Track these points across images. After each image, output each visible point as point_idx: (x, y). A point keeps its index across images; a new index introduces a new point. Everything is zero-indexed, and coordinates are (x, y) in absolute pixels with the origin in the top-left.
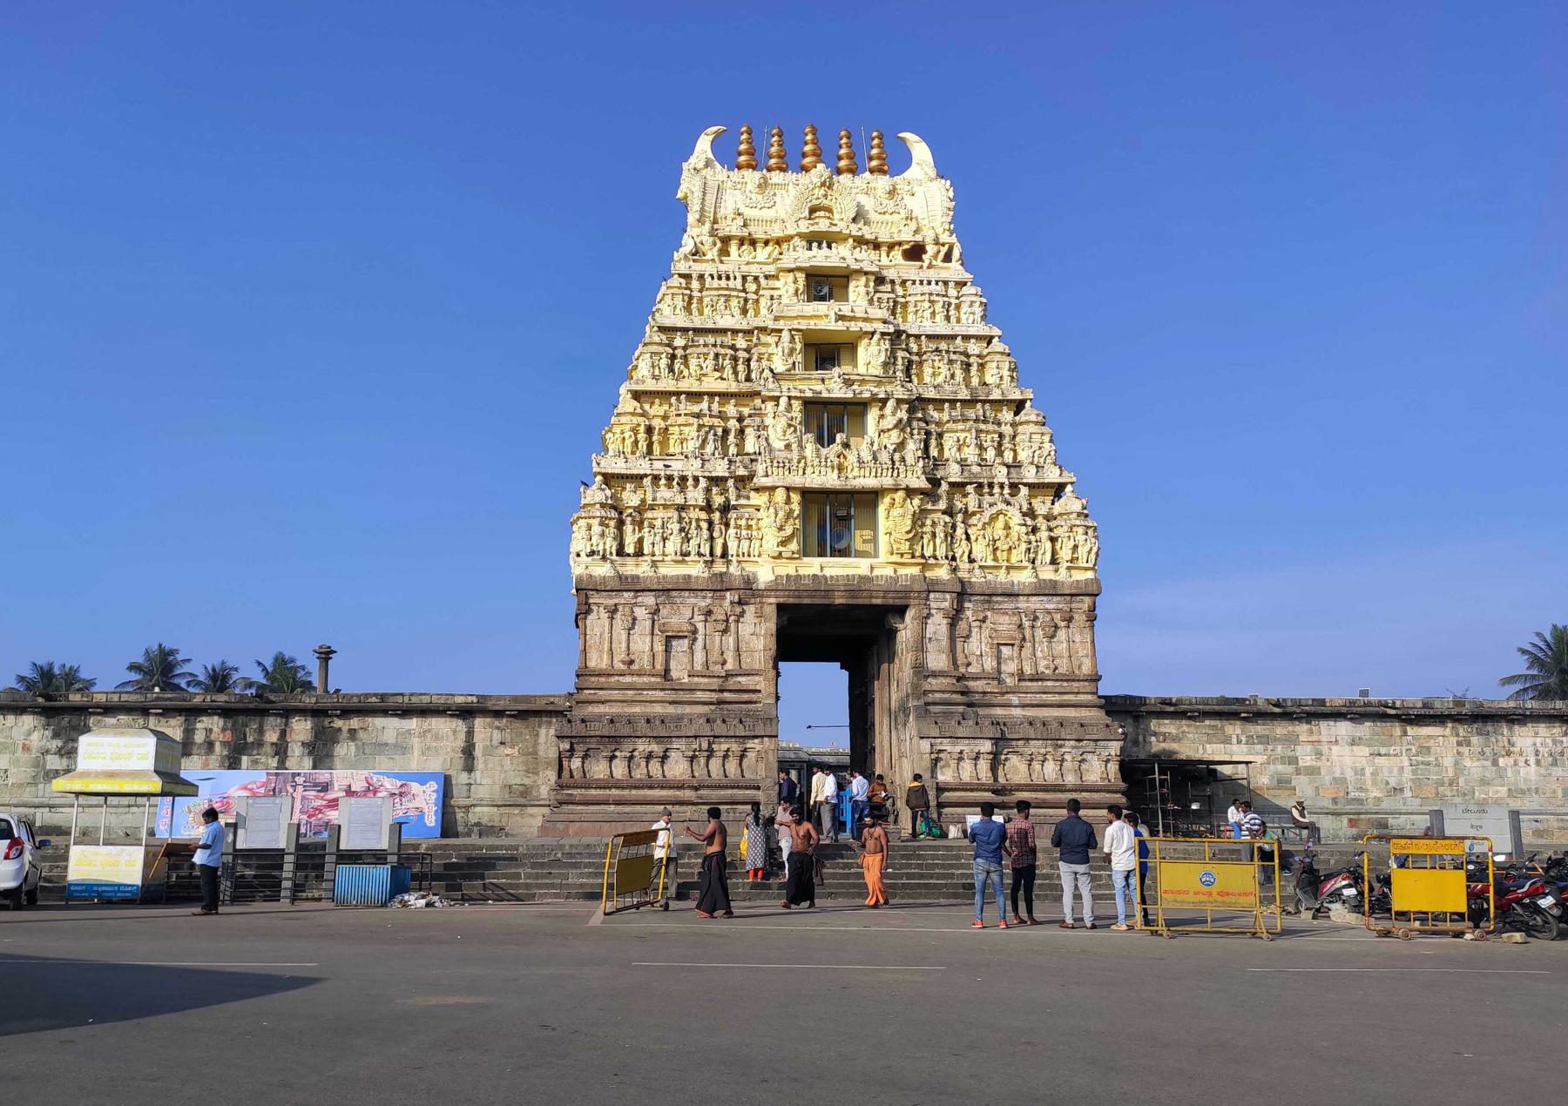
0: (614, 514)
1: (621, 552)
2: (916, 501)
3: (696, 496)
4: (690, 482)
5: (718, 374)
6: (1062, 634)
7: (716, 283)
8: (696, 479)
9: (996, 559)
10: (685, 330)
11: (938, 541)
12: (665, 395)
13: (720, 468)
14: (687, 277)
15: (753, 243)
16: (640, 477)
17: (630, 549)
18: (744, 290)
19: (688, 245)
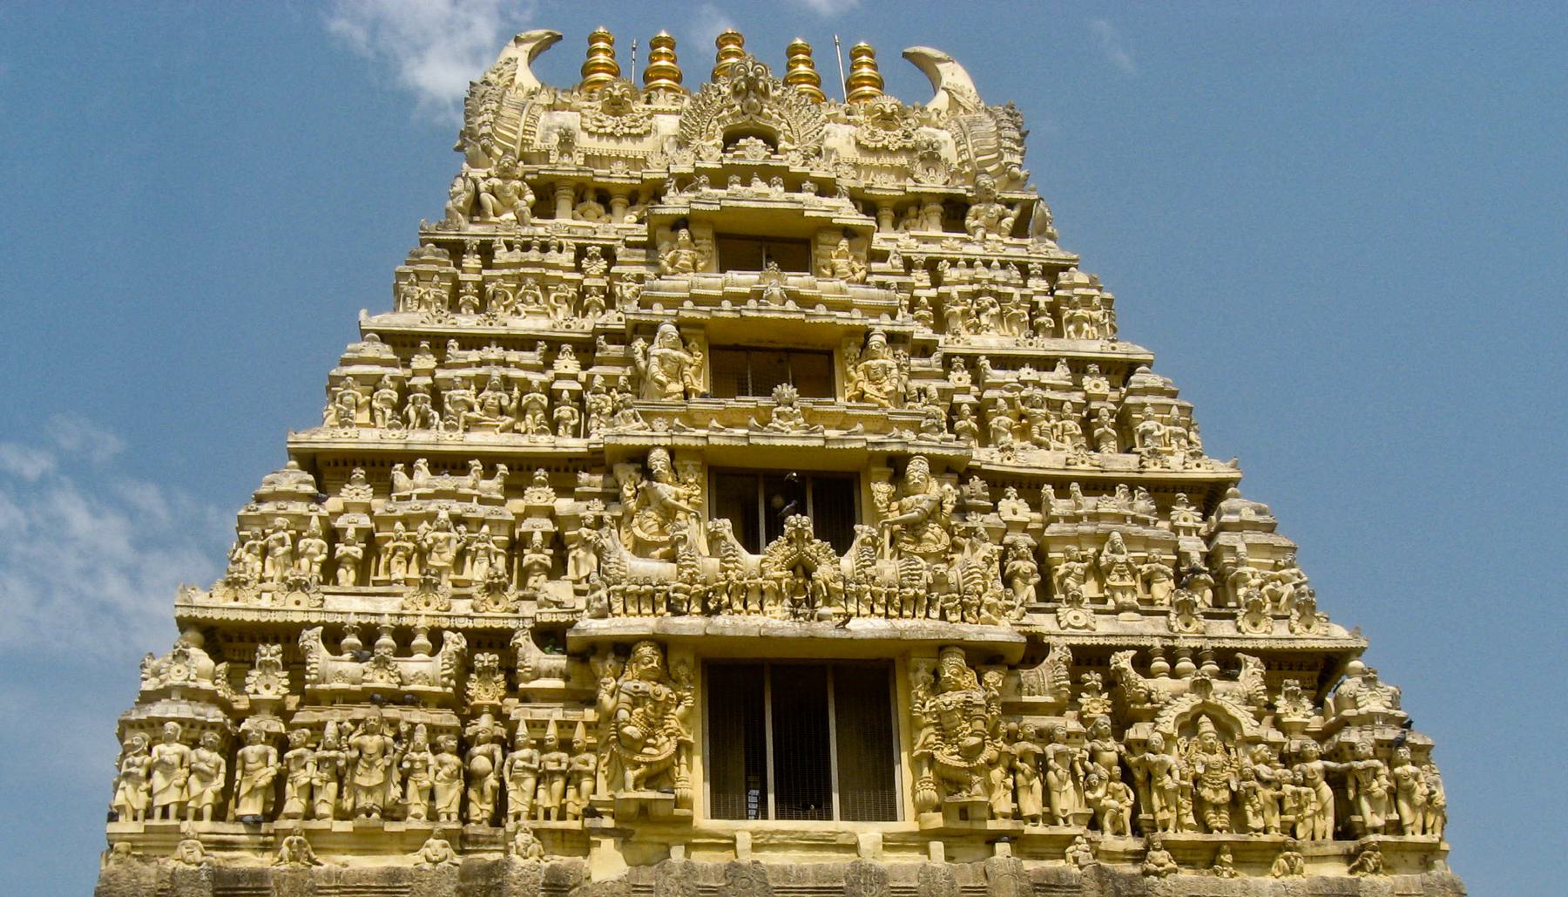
4: (421, 640)
8: (436, 637)
15: (604, 198)
16: (287, 635)
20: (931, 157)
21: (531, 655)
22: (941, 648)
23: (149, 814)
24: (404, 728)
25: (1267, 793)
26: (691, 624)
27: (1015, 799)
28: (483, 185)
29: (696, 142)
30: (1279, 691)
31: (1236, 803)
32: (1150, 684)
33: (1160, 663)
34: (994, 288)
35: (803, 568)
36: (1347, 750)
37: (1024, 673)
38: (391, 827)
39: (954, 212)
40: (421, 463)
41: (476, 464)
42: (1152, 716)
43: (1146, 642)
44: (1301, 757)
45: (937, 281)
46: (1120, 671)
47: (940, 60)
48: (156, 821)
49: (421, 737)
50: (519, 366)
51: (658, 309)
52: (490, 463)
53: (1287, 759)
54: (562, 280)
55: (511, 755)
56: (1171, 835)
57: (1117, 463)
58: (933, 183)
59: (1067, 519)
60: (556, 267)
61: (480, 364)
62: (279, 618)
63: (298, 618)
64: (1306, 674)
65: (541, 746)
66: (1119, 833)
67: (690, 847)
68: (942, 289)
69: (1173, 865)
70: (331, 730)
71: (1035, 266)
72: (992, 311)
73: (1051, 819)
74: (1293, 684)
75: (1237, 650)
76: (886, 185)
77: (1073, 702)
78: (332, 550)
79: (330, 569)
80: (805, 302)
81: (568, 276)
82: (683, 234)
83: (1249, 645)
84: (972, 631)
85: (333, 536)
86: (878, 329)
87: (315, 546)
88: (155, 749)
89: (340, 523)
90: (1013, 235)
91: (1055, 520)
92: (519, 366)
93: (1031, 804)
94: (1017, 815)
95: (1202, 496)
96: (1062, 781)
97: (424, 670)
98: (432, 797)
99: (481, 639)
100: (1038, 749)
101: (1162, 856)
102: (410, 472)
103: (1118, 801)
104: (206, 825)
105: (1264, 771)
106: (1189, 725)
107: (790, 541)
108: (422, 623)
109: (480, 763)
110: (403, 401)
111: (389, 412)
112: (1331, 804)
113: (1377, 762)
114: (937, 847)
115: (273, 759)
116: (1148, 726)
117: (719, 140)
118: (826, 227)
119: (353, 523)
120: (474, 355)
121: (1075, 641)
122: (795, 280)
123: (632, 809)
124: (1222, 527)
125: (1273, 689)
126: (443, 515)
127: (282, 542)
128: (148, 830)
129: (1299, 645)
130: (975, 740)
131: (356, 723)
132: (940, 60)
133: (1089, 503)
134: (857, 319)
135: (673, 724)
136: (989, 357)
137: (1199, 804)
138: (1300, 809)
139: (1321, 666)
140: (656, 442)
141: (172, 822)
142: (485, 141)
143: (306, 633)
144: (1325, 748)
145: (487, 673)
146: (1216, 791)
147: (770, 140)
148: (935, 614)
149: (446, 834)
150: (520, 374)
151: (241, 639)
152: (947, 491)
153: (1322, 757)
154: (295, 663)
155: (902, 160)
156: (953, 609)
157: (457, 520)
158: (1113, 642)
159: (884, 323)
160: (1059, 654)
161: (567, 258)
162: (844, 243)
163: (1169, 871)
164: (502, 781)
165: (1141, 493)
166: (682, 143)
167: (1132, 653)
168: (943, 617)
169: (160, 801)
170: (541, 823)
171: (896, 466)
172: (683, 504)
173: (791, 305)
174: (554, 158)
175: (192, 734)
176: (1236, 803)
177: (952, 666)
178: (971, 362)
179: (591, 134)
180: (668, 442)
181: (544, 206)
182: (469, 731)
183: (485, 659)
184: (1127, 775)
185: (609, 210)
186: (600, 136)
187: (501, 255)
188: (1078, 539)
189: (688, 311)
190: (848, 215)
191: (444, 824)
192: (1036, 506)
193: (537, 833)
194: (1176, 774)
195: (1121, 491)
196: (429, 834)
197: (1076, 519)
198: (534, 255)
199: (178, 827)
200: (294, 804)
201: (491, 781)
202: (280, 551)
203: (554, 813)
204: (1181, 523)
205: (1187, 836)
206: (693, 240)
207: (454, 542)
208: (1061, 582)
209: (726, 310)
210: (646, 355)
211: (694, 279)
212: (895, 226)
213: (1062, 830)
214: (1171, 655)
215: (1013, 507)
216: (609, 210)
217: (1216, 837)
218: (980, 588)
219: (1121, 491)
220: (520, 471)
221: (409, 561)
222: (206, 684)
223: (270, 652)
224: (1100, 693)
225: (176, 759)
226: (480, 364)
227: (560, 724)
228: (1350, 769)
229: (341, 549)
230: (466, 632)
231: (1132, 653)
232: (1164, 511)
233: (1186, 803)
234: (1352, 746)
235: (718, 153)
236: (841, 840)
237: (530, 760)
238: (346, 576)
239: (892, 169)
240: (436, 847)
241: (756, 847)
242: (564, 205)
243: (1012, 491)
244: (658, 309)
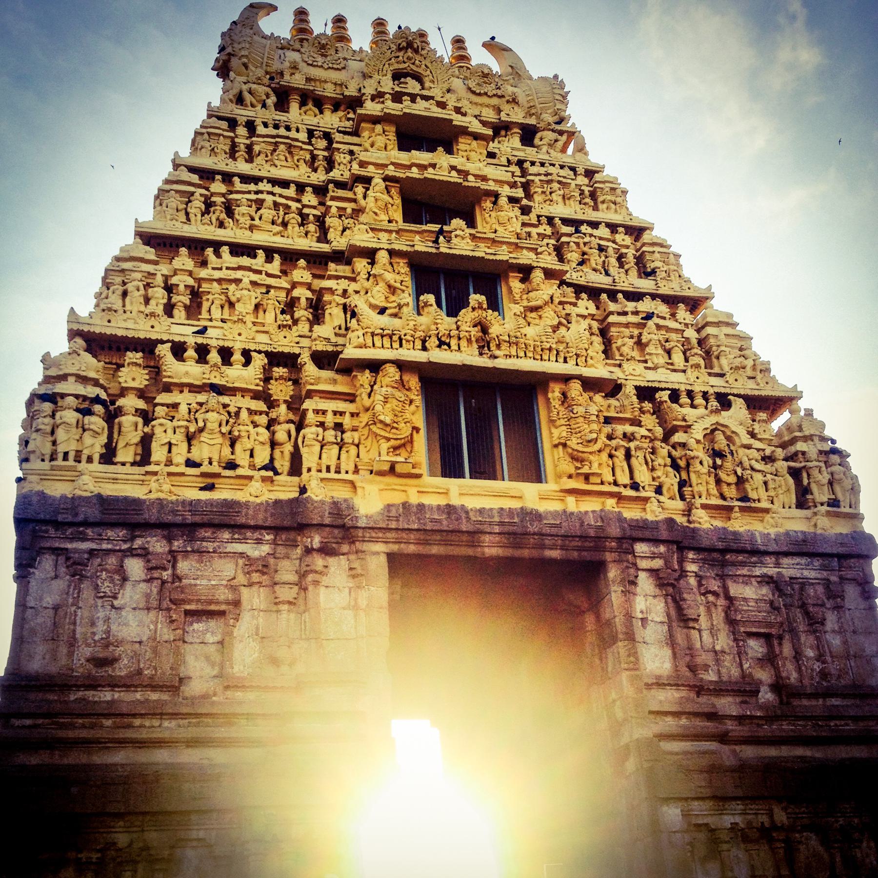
4: (237, 357)
16: (148, 347)
21: (310, 370)
22: (566, 379)
24: (232, 409)
25: (758, 477)
33: (684, 400)
40: (225, 249)
41: (261, 253)
42: (687, 429)
43: (676, 386)
48: (60, 462)
49: (244, 414)
50: (281, 196)
51: (371, 168)
52: (270, 252)
54: (302, 149)
58: (517, 116)
59: (619, 314)
60: (297, 140)
61: (257, 193)
62: (142, 336)
63: (154, 337)
65: (322, 425)
66: (672, 498)
70: (183, 409)
71: (580, 170)
79: (169, 309)
83: (736, 392)
85: (169, 289)
87: (159, 294)
88: (58, 415)
89: (174, 280)
91: (612, 313)
92: (281, 196)
94: (615, 483)
97: (240, 375)
98: (252, 456)
99: (275, 359)
102: (218, 255)
104: (96, 466)
105: (757, 466)
107: (474, 309)
112: (793, 487)
115: (140, 426)
118: (464, 131)
120: (252, 187)
123: (386, 467)
126: (246, 281)
129: (763, 393)
130: (594, 436)
131: (201, 404)
133: (631, 306)
134: (491, 186)
136: (561, 219)
137: (718, 481)
141: (71, 462)
142: (245, 60)
148: (561, 360)
150: (283, 201)
153: (786, 459)
155: (495, 101)
157: (254, 283)
158: (656, 385)
168: (565, 361)
170: (324, 475)
171: (525, 272)
172: (398, 285)
174: (287, 77)
178: (550, 220)
182: (273, 415)
185: (321, 112)
187: (261, 130)
188: (627, 325)
189: (391, 171)
193: (322, 480)
196: (250, 478)
197: (625, 313)
200: (158, 453)
203: (333, 469)
208: (618, 349)
209: (415, 173)
213: (643, 494)
214: (690, 394)
216: (321, 112)
220: (290, 257)
221: (222, 307)
222: (92, 375)
225: (74, 421)
226: (257, 193)
229: (175, 299)
230: (268, 354)
233: (712, 480)
234: (804, 453)
238: (180, 314)
242: (294, 106)
244: (371, 168)
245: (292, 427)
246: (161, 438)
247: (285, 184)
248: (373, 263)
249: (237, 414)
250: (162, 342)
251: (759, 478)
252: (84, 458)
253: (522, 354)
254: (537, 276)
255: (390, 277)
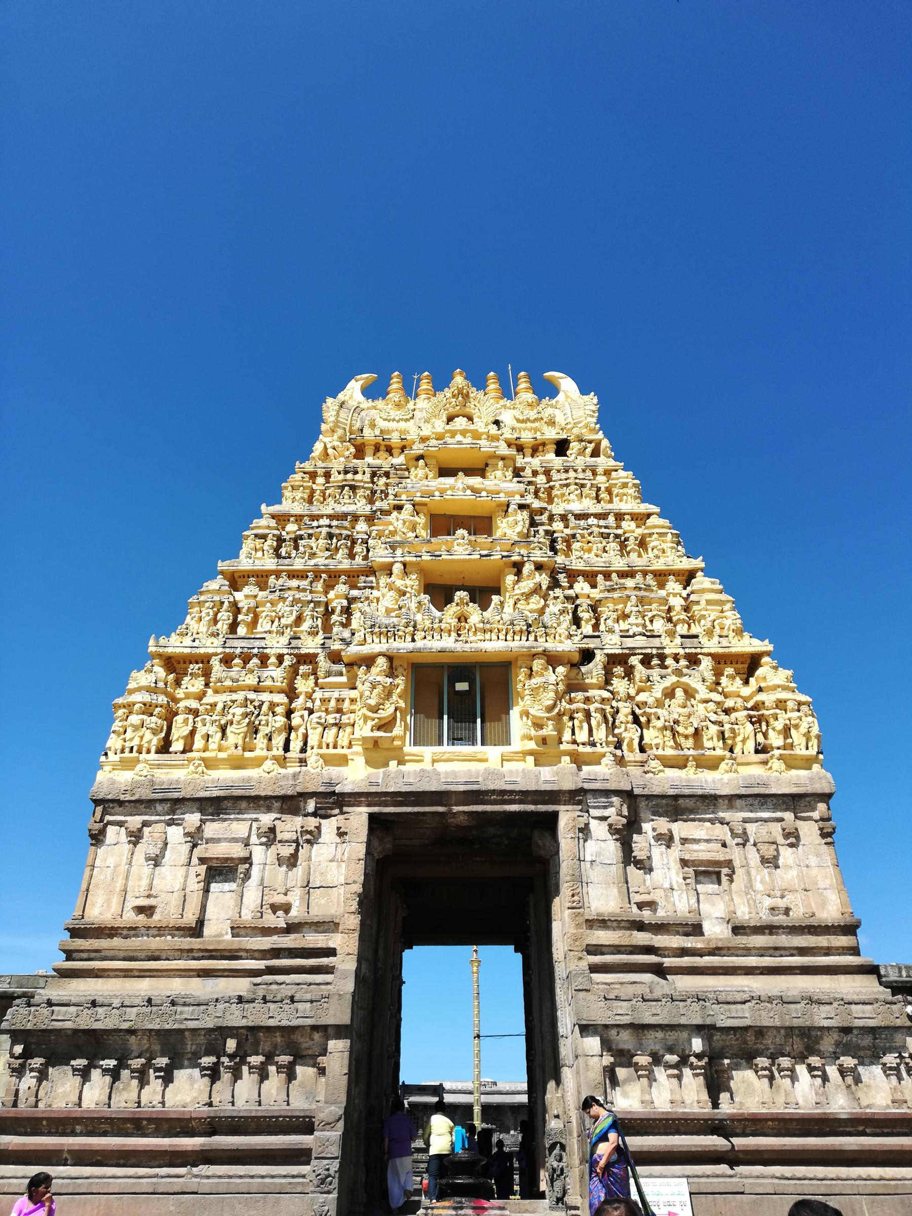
0: (162, 699)
1: (165, 747)
2: (561, 670)
3: (276, 674)
4: (273, 660)
5: (328, 554)
6: (787, 855)
7: (341, 477)
8: (280, 658)
9: (678, 746)
10: (299, 518)
11: (593, 722)
12: (261, 578)
13: (310, 645)
14: (313, 475)
16: (205, 660)
17: (177, 746)
18: (373, 483)
19: (318, 447)
20: (552, 423)
23: (123, 751)
24: (257, 704)
26: (403, 645)
27: (573, 733)
28: (328, 446)
29: (433, 420)
30: (723, 675)
31: (697, 733)
32: (649, 671)
33: (655, 662)
34: (577, 481)
35: (462, 618)
36: (761, 705)
37: (584, 669)
38: (247, 754)
39: (562, 447)
43: (649, 651)
44: (734, 709)
45: (549, 480)
46: (632, 667)
47: (561, 378)
48: (127, 754)
53: (727, 712)
54: (363, 487)
55: (311, 716)
56: (660, 752)
57: (636, 560)
58: (551, 434)
63: (211, 651)
64: (740, 666)
67: (401, 762)
68: (551, 484)
69: (662, 768)
71: (600, 470)
72: (577, 492)
73: (593, 744)
74: (729, 670)
75: (697, 654)
76: (527, 437)
77: (608, 682)
78: (235, 618)
80: (475, 491)
81: (366, 485)
82: (421, 462)
83: (705, 651)
84: (552, 645)
86: (513, 502)
87: (225, 616)
90: (592, 456)
93: (582, 736)
94: (574, 742)
95: (684, 578)
96: (599, 725)
98: (270, 739)
100: (586, 707)
101: (655, 764)
103: (631, 734)
104: (153, 756)
106: (670, 694)
107: (457, 604)
108: (273, 651)
109: (296, 720)
110: (279, 547)
111: (271, 551)
113: (778, 711)
114: (530, 759)
115: (191, 721)
116: (647, 694)
117: (445, 419)
119: (244, 604)
121: (610, 652)
122: (475, 481)
124: (692, 593)
125: (718, 674)
127: (208, 614)
128: (122, 760)
129: (733, 650)
131: (233, 702)
132: (561, 378)
135: (395, 697)
137: (674, 734)
138: (734, 738)
139: (749, 661)
140: (396, 559)
141: (135, 754)
143: (214, 658)
144: (749, 705)
145: (306, 676)
146: (686, 728)
147: (470, 419)
149: (275, 758)
151: (185, 663)
152: (543, 579)
153: (746, 709)
154: (207, 674)
155: (537, 424)
156: (541, 636)
159: (517, 499)
160: (600, 657)
161: (367, 477)
162: (501, 463)
163: (660, 771)
164: (306, 729)
165: (649, 577)
166: (427, 421)
167: (641, 657)
168: (536, 640)
169: (128, 744)
170: (324, 751)
172: (409, 589)
173: (469, 492)
175: (148, 709)
176: (697, 733)
177: (537, 664)
179: (385, 420)
180: (402, 559)
181: (360, 453)
183: (303, 669)
184: (636, 720)
186: (389, 421)
190: (503, 450)
191: (275, 752)
192: (594, 586)
193: (322, 756)
194: (662, 719)
195: (639, 577)
198: (350, 476)
199: (138, 758)
200: (199, 743)
201: (302, 730)
202: (208, 618)
203: (331, 746)
204: (671, 591)
205: (669, 752)
206: (426, 465)
207: (295, 612)
210: (398, 520)
211: (422, 482)
212: (532, 456)
213: (599, 749)
214: (662, 657)
215: (581, 587)
217: (686, 752)
218: (555, 625)
219: (639, 577)
223: (194, 668)
224: (624, 678)
227: (338, 700)
228: (763, 715)
229: (240, 617)
231: (641, 657)
232: (662, 586)
233: (668, 733)
235: (443, 425)
236: (479, 756)
237: (320, 718)
239: (530, 430)
240: (268, 765)
241: (434, 761)
243: (580, 578)
245: (306, 713)
246: (201, 730)
247: (343, 517)
248: (390, 574)
249: (260, 707)
250: (216, 654)
251: (714, 729)
252: (144, 750)
253: (494, 637)
254: (528, 568)
255: (399, 583)
